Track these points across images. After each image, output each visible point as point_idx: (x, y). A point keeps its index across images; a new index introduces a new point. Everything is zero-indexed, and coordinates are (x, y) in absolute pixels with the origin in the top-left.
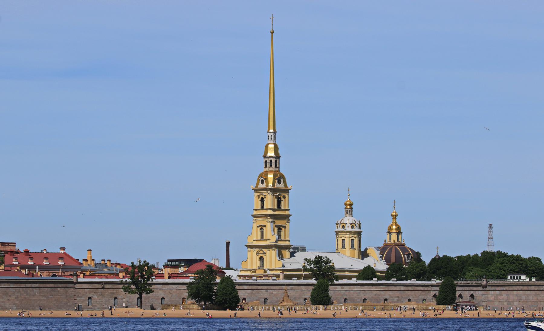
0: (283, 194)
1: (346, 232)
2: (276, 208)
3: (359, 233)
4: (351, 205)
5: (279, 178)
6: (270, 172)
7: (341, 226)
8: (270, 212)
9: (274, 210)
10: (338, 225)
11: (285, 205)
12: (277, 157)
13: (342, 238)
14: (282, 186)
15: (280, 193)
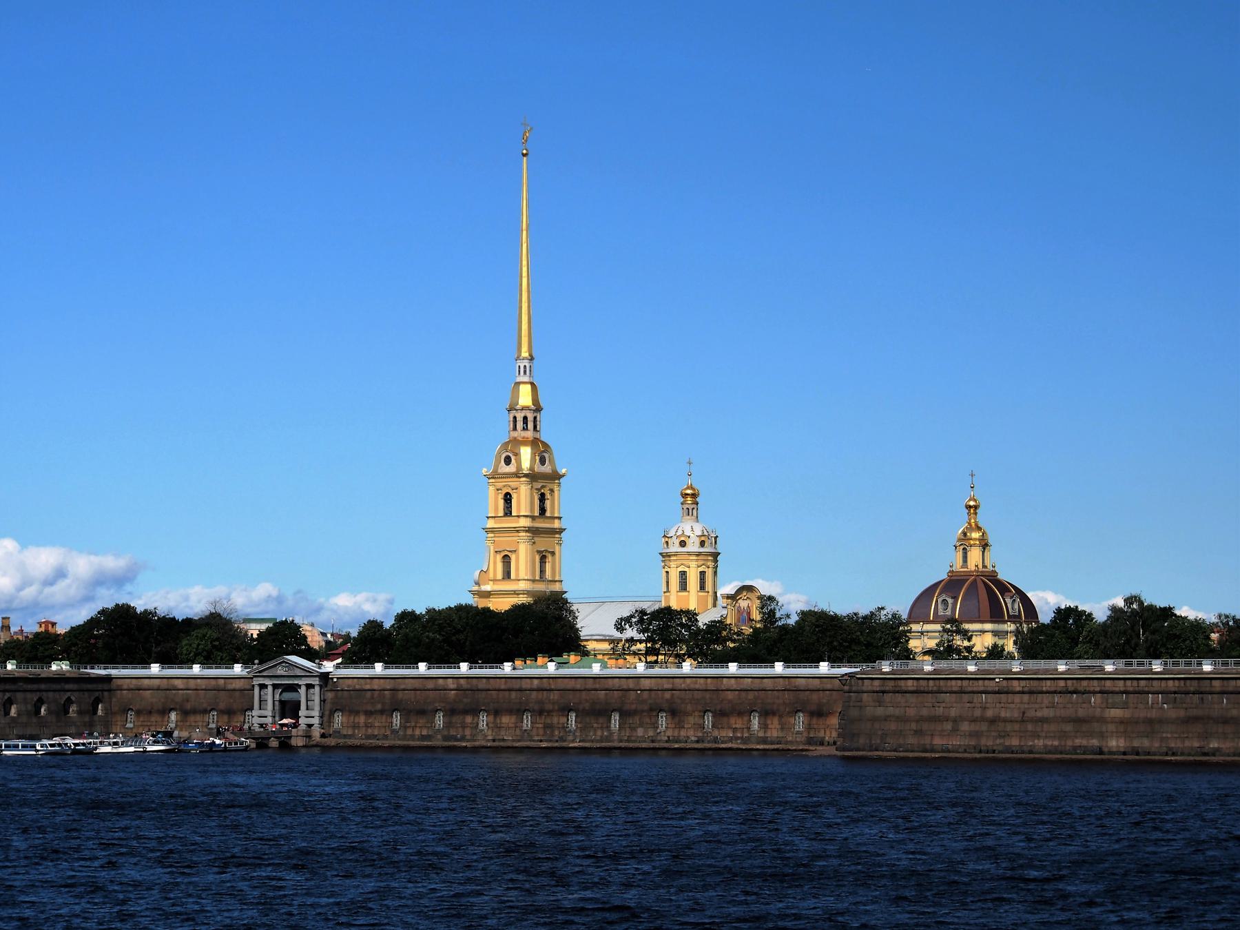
0: (513, 483)
1: (689, 554)
2: (537, 513)
3: (715, 556)
4: (694, 496)
5: (542, 451)
6: (524, 442)
7: (677, 542)
8: (524, 522)
9: (533, 518)
10: (670, 541)
11: (519, 510)
12: (538, 409)
13: (681, 569)
14: (547, 468)
15: (544, 481)
